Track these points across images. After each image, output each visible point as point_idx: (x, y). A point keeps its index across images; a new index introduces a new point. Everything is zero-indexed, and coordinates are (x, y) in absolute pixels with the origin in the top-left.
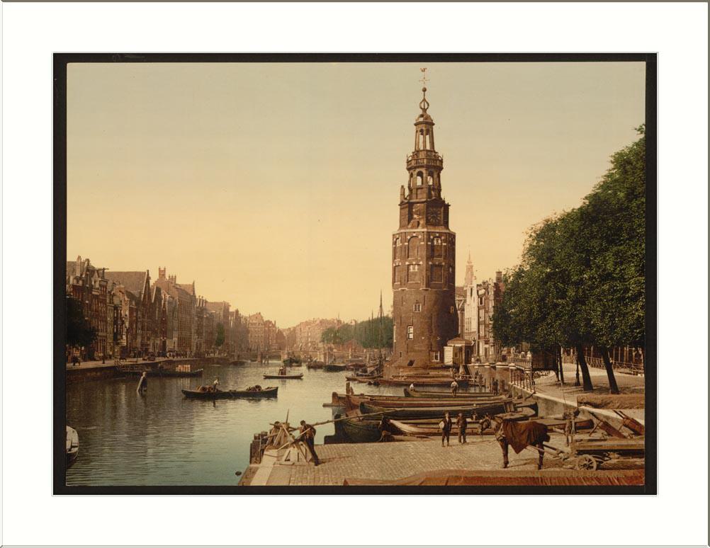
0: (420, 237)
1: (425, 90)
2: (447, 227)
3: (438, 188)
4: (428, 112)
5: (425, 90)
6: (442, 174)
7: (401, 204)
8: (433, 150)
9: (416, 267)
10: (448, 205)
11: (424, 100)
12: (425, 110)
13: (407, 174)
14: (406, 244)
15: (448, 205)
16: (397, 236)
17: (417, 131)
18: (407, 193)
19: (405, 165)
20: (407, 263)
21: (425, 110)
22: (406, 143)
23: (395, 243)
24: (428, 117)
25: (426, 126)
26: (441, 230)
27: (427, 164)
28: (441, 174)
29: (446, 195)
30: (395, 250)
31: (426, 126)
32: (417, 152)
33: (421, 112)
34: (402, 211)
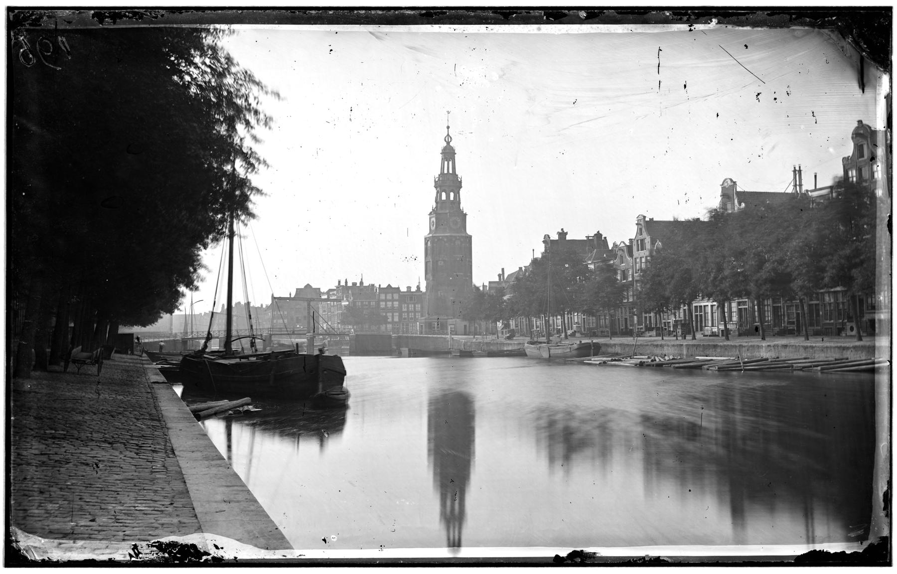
1: (448, 127)
3: (457, 201)
4: (451, 144)
5: (448, 127)
6: (462, 191)
8: (454, 174)
10: (466, 215)
12: (448, 143)
13: (434, 192)
15: (466, 215)
19: (433, 184)
21: (448, 143)
22: (434, 167)
23: (426, 244)
25: (449, 154)
27: (448, 183)
29: (465, 206)
31: (449, 154)
32: (442, 174)
33: (445, 144)
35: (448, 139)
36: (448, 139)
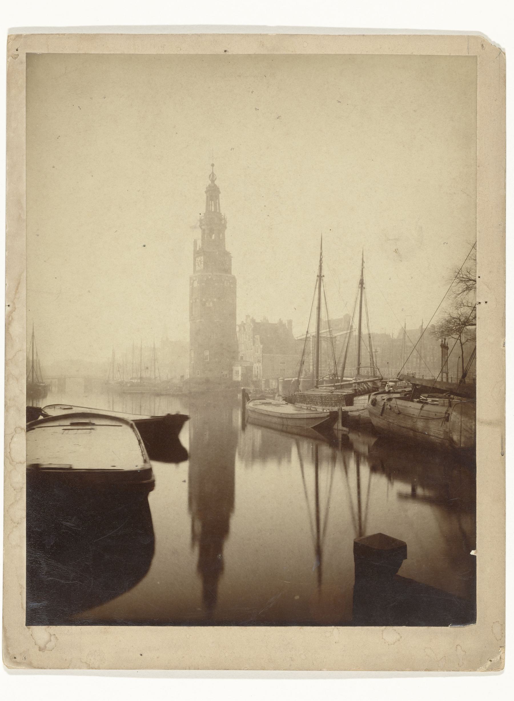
0: (214, 279)
1: (213, 165)
2: (231, 274)
4: (216, 182)
7: (197, 253)
9: (211, 304)
11: (213, 173)
12: (213, 181)
14: (203, 284)
16: (195, 279)
17: (207, 197)
18: (199, 243)
20: (204, 300)
21: (213, 181)
23: (192, 284)
24: (215, 185)
26: (229, 275)
27: (213, 225)
28: (225, 234)
30: (192, 289)
33: (210, 182)
34: (197, 259)
35: (213, 177)
36: (213, 177)
